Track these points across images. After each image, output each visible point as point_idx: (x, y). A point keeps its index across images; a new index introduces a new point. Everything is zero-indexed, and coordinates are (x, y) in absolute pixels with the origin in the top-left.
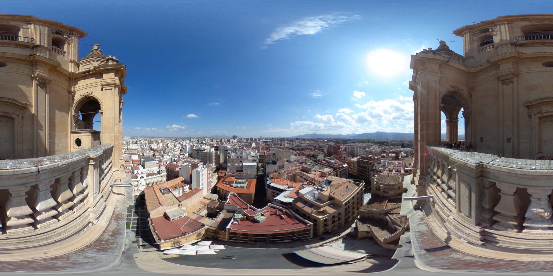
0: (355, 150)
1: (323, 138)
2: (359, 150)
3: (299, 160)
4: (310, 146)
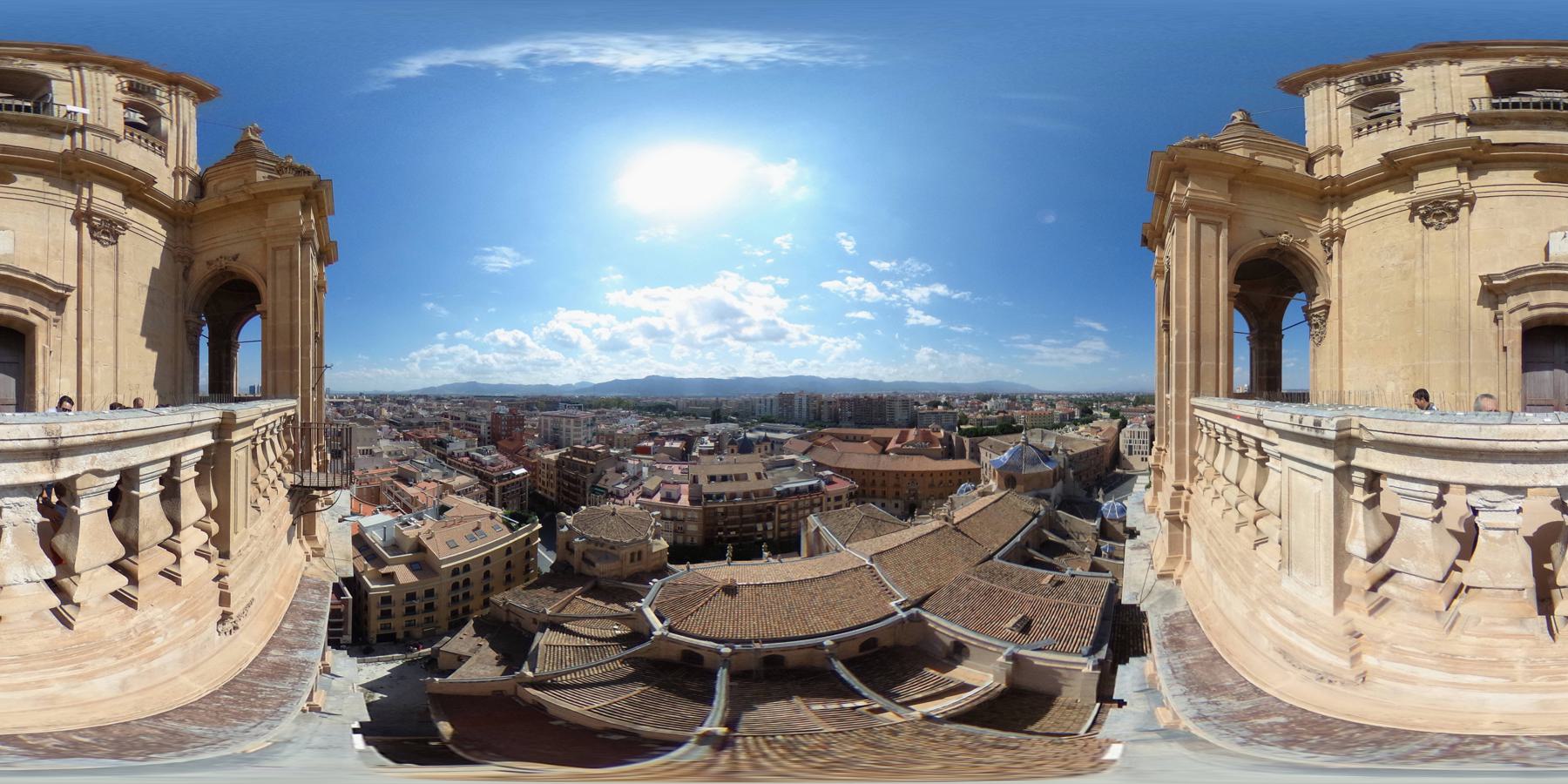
0: (564, 429)
1: (489, 395)
2: (575, 430)
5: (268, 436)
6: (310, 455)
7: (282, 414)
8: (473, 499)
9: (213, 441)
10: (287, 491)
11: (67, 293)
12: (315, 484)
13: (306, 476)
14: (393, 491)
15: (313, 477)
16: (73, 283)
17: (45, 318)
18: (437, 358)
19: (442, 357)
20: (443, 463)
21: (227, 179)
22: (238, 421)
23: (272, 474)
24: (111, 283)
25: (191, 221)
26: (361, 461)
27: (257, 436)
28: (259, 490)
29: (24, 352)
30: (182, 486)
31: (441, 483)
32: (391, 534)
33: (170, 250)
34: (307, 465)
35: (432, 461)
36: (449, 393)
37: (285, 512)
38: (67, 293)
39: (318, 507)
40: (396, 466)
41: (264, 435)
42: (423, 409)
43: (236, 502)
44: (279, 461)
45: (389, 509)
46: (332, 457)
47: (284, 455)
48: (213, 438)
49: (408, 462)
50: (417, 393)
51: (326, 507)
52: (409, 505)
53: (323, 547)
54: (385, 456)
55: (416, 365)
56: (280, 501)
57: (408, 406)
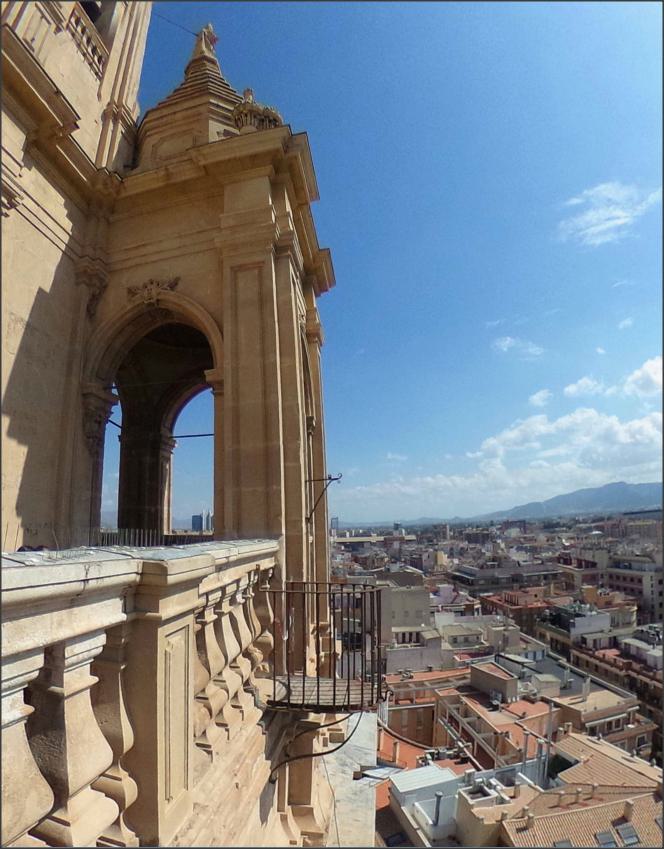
3: (470, 639)
4: (567, 561)
5: (226, 607)
6: (304, 642)
7: (252, 566)
8: (622, 746)
9: (123, 617)
10: (260, 713)
12: (312, 700)
13: (296, 684)
14: (458, 717)
15: (309, 687)
18: (537, 445)
19: (548, 441)
20: (563, 661)
21: (172, 136)
22: (171, 580)
23: (233, 681)
25: (113, 212)
26: (398, 654)
27: (205, 607)
28: (210, 711)
30: (67, 704)
31: (557, 705)
32: (450, 812)
33: (73, 257)
34: (297, 663)
35: (539, 657)
36: (570, 512)
37: (258, 754)
39: (317, 746)
40: (467, 665)
41: (218, 605)
42: (519, 549)
43: (167, 734)
44: (247, 654)
45: (450, 757)
46: (345, 647)
47: (256, 643)
48: (125, 612)
49: (491, 659)
50: (505, 518)
51: (331, 746)
52: (489, 750)
53: (323, 832)
54: (446, 646)
55: (498, 463)
56: (248, 732)
57: (489, 546)
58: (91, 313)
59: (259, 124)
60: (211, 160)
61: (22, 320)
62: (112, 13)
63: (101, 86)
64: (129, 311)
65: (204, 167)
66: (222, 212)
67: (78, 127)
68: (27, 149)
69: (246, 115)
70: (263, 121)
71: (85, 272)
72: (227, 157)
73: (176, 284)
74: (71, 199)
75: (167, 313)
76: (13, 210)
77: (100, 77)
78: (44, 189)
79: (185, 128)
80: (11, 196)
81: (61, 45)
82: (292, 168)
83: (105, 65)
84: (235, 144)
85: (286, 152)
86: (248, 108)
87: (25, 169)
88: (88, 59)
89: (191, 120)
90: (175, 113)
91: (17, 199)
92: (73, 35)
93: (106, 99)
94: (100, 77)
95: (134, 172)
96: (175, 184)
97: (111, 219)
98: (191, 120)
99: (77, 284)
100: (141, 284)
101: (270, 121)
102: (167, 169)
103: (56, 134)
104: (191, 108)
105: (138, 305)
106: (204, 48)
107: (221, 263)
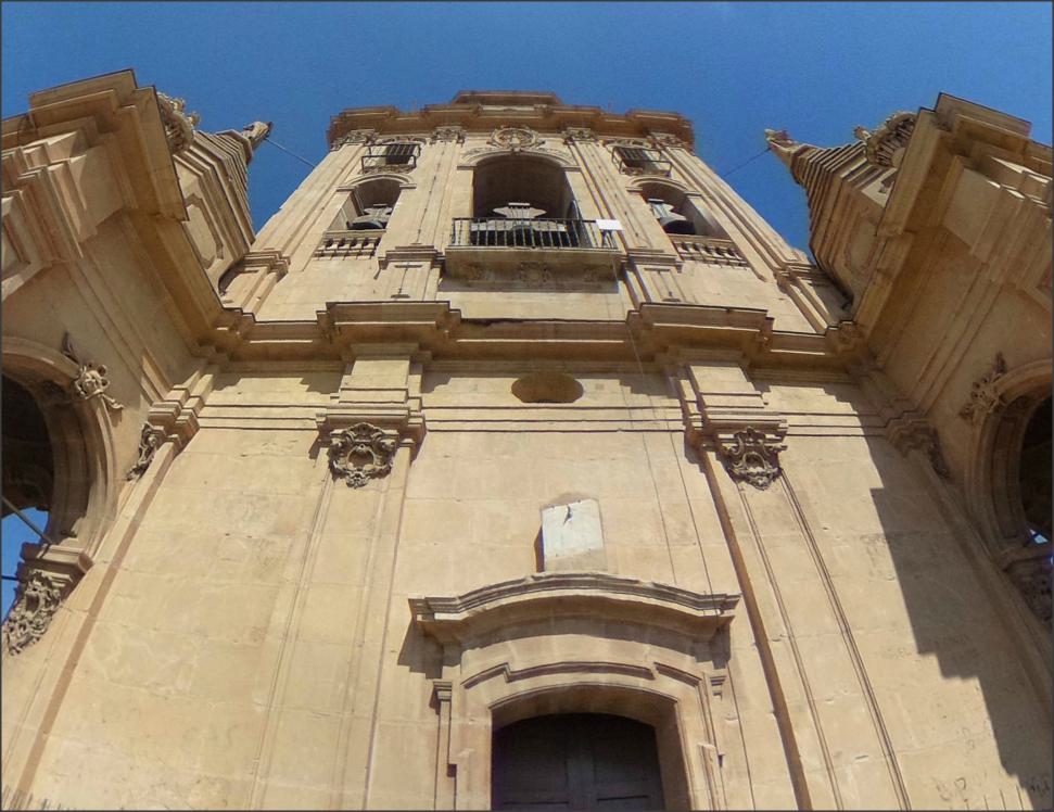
11: (727, 613)
16: (733, 588)
17: (692, 681)
24: (809, 563)
25: (874, 357)
29: (657, 769)
38: (727, 613)
58: (943, 472)
59: (900, 141)
60: (904, 219)
61: (877, 535)
62: (699, 213)
63: (753, 269)
64: (982, 435)
65: (907, 230)
66: (969, 248)
67: (772, 319)
68: (751, 378)
69: (882, 149)
70: (898, 135)
71: (902, 436)
72: (913, 199)
73: (1003, 362)
74: (827, 383)
75: (1023, 401)
76: (786, 438)
77: (745, 264)
78: (796, 396)
79: (852, 223)
80: (773, 428)
81: (693, 275)
82: (974, 135)
83: (738, 252)
84: (905, 180)
85: (949, 130)
86: (875, 142)
87: (765, 395)
88: (723, 263)
89: (848, 209)
90: (830, 221)
91: (782, 425)
92: (692, 259)
93: (769, 274)
94: (745, 264)
95: (855, 303)
96: (900, 274)
97: (880, 365)
98: (848, 209)
99: (905, 455)
100: (969, 397)
101: (904, 127)
102: (879, 271)
103: (761, 343)
104: (836, 201)
105: (986, 421)
106: (786, 150)
107: (1023, 295)
